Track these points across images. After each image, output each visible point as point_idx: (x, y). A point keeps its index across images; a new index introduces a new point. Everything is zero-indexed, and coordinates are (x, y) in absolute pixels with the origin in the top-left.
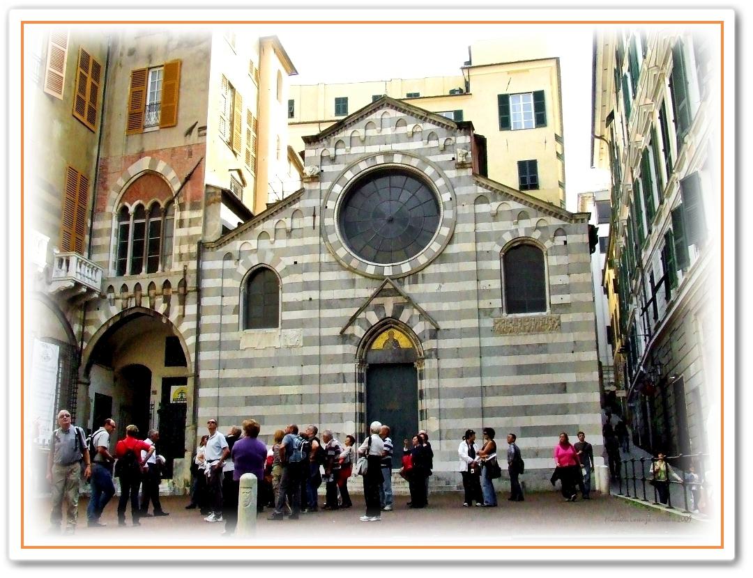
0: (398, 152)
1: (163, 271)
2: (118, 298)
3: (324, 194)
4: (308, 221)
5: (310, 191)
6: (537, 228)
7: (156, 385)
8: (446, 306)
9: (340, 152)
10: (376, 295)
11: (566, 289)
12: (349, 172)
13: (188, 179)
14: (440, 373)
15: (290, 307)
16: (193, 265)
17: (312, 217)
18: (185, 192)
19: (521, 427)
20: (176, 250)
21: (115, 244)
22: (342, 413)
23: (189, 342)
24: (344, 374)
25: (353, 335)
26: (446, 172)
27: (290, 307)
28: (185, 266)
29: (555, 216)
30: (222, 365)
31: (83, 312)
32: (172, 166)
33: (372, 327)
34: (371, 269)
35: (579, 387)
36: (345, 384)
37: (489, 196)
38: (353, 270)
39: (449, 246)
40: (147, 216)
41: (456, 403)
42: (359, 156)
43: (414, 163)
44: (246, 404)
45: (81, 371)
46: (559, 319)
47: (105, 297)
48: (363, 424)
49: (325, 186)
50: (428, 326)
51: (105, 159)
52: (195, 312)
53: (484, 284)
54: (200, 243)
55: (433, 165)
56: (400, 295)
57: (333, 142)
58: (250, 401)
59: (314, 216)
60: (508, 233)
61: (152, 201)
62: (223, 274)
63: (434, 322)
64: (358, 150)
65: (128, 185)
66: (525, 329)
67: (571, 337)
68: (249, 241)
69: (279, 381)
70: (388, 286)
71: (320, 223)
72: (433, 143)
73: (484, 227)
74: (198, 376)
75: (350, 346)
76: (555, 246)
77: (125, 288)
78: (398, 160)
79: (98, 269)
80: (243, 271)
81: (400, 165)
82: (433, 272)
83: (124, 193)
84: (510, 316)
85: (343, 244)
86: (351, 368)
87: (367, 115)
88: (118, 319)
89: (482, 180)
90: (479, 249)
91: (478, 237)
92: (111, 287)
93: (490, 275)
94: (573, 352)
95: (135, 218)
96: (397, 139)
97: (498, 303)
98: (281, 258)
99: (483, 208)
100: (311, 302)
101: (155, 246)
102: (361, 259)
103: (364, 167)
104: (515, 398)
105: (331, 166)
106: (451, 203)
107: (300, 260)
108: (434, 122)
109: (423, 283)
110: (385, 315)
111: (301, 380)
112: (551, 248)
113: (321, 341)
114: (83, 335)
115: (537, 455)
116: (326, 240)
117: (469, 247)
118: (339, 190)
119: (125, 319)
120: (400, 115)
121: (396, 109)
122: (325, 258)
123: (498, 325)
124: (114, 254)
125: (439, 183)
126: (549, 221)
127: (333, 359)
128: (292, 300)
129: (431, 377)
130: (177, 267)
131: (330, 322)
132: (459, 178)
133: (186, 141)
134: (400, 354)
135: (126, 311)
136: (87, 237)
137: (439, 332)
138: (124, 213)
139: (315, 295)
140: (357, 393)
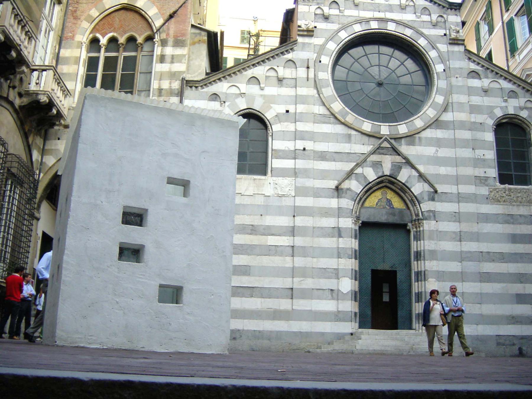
3: (317, 49)
4: (302, 72)
5: (304, 44)
8: (443, 170)
9: (334, 12)
10: (374, 152)
12: (343, 31)
13: (171, 16)
14: (441, 235)
18: (168, 29)
20: (155, 85)
21: (82, 73)
22: (337, 270)
25: (349, 189)
33: (370, 183)
34: (367, 126)
36: (340, 239)
37: (480, 73)
40: (121, 49)
42: (354, 19)
43: (408, 32)
49: (317, 41)
50: (427, 187)
53: (479, 153)
59: (308, 68)
63: (432, 186)
65: (102, 16)
66: (517, 200)
70: (386, 145)
71: (315, 75)
72: (426, 18)
73: (476, 100)
78: (391, 28)
83: (97, 24)
85: (338, 99)
91: (474, 109)
93: (482, 144)
95: (107, 50)
97: (493, 173)
98: (272, 105)
99: (475, 83)
100: (305, 152)
103: (358, 29)
106: (444, 73)
109: (420, 145)
110: (383, 172)
111: (293, 231)
113: (317, 193)
117: (462, 116)
118: (333, 47)
125: (432, 54)
127: (326, 213)
128: (284, 149)
131: (324, 175)
134: (394, 215)
137: (436, 196)
139: (309, 145)
140: (354, 250)
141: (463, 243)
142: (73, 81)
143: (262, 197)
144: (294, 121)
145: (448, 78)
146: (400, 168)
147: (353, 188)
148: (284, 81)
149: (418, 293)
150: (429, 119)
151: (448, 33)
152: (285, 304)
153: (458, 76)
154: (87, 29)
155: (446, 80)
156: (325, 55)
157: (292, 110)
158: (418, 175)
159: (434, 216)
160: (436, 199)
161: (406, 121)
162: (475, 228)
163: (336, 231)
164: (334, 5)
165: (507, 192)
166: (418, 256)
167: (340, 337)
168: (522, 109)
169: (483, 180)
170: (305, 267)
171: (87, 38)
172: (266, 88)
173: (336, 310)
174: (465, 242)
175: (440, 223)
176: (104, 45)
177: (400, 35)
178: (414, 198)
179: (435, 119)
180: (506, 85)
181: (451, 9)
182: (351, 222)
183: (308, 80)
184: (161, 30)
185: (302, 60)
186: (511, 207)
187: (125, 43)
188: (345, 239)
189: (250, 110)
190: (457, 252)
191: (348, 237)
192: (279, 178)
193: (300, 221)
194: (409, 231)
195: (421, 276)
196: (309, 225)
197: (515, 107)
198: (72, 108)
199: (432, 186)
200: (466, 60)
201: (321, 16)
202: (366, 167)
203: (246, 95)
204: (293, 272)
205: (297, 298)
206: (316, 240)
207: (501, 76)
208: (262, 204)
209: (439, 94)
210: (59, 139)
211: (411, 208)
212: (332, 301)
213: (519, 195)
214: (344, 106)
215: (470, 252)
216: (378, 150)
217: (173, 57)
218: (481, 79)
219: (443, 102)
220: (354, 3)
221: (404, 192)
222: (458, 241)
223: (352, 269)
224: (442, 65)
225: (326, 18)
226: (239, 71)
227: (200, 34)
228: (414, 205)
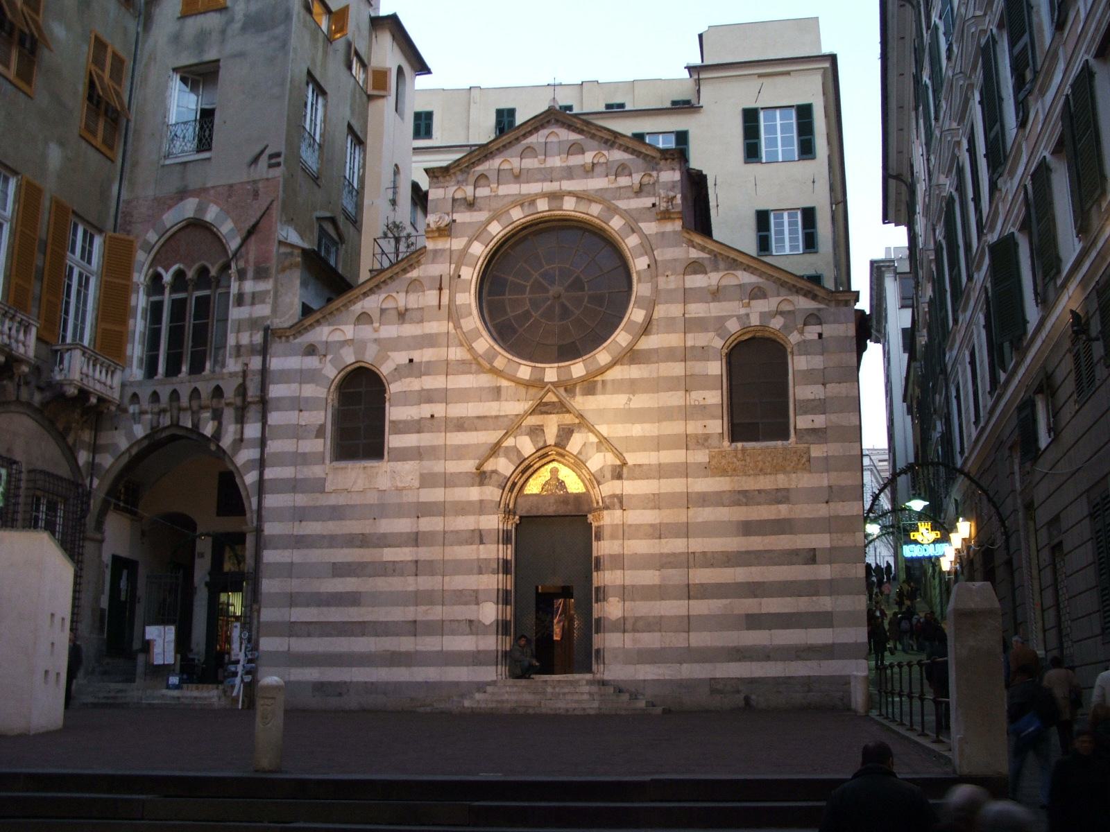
0: (570, 193)
1: (213, 372)
3: (455, 257)
4: (431, 297)
5: (436, 252)
6: (779, 313)
8: (637, 430)
9: (483, 192)
10: (533, 412)
13: (251, 232)
14: (624, 531)
16: (256, 363)
17: (438, 292)
18: (247, 253)
20: (231, 340)
21: (142, 329)
22: (476, 591)
23: (250, 478)
24: (480, 531)
25: (495, 472)
26: (642, 225)
29: (805, 295)
31: (93, 433)
32: (228, 213)
33: (525, 459)
34: (525, 371)
36: (482, 547)
37: (706, 263)
40: (190, 288)
41: (649, 577)
43: (595, 209)
44: (334, 576)
45: (90, 520)
47: (125, 411)
48: (509, 607)
49: (457, 244)
51: (128, 202)
52: (259, 435)
54: (266, 329)
55: (625, 214)
56: (568, 412)
58: (340, 570)
59: (440, 289)
60: (735, 318)
61: (196, 266)
63: (619, 455)
65: (162, 240)
68: (341, 327)
70: (551, 398)
72: (624, 181)
73: (697, 310)
74: (262, 531)
76: (804, 341)
77: (155, 397)
78: (569, 205)
80: (331, 372)
81: (573, 213)
82: (619, 377)
83: (158, 252)
88: (146, 443)
89: (698, 239)
90: (689, 344)
91: (690, 325)
92: (135, 398)
94: (827, 502)
96: (569, 173)
97: (716, 426)
101: (201, 334)
102: (510, 357)
105: (468, 214)
109: (603, 393)
110: (545, 441)
112: (798, 344)
113: (447, 481)
114: (93, 467)
116: (458, 326)
117: (673, 340)
118: (479, 250)
119: (156, 444)
120: (574, 136)
122: (456, 353)
124: (140, 347)
125: (631, 242)
126: (796, 303)
131: (460, 452)
132: (663, 234)
138: (155, 283)
139: (439, 410)
140: (501, 561)
141: (663, 541)
147: (501, 470)
151: (657, 204)
153: (669, 273)
154: (144, 263)
158: (596, 440)
159: (621, 502)
160: (625, 476)
161: (584, 358)
163: (477, 535)
164: (482, 182)
167: (481, 687)
170: (433, 590)
171: (146, 275)
172: (382, 327)
173: (475, 650)
174: (666, 540)
177: (583, 215)
178: (592, 477)
181: (666, 159)
183: (440, 308)
184: (238, 255)
185: (432, 278)
186: (744, 478)
187: (195, 277)
188: (488, 546)
190: (656, 554)
195: (601, 594)
196: (438, 529)
197: (762, 315)
199: (619, 455)
200: (684, 245)
201: (463, 202)
202: (521, 435)
203: (355, 341)
206: (448, 549)
208: (376, 502)
209: (639, 307)
210: (116, 429)
212: (470, 637)
215: (674, 554)
216: (539, 408)
217: (254, 295)
218: (706, 273)
220: (513, 174)
223: (498, 590)
226: (343, 306)
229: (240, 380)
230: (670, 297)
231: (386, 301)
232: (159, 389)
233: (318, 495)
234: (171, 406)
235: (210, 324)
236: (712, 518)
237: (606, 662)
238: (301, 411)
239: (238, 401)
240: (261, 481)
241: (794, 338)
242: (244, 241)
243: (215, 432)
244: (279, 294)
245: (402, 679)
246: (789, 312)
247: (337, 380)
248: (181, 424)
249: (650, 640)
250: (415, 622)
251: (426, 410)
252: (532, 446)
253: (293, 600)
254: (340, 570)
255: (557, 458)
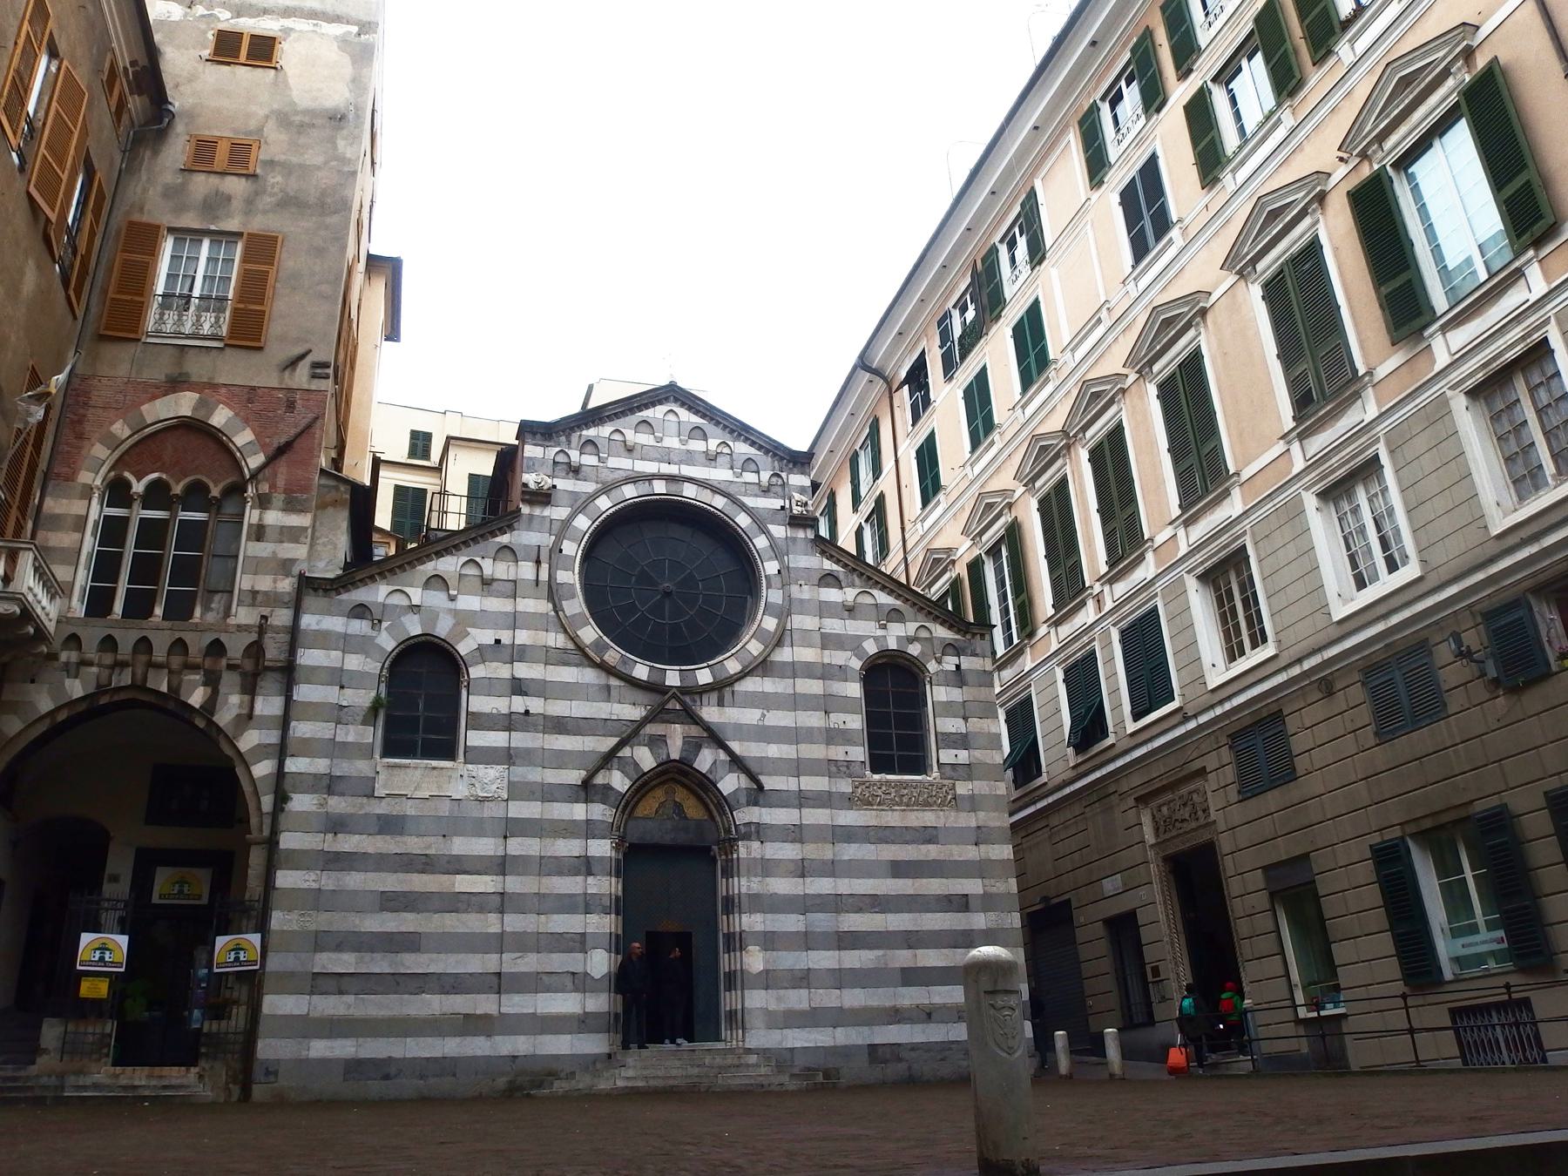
0: (691, 480)
2: (90, 664)
3: (556, 527)
4: (526, 570)
7: (120, 864)
8: (773, 751)
9: (589, 460)
11: (962, 741)
12: (604, 497)
14: (767, 868)
15: (481, 722)
16: (282, 617)
18: (275, 475)
19: (903, 969)
20: (244, 582)
22: (584, 935)
23: (262, 769)
24: (587, 857)
25: (608, 788)
27: (481, 722)
28: (264, 617)
30: (336, 825)
32: (246, 421)
33: (645, 774)
34: (641, 671)
35: (988, 902)
36: (590, 880)
37: (841, 577)
38: (603, 667)
39: (778, 650)
41: (791, 923)
42: (623, 474)
43: (719, 502)
44: (383, 909)
46: (953, 788)
47: (53, 657)
49: (559, 513)
51: (84, 379)
53: (837, 719)
57: (575, 437)
58: (392, 902)
59: (538, 562)
62: (346, 643)
63: (753, 777)
64: (623, 463)
66: (902, 800)
67: (968, 820)
69: (459, 866)
70: (674, 705)
72: (750, 477)
73: (834, 626)
74: (278, 843)
75: (602, 806)
77: (109, 643)
78: (689, 491)
79: (56, 593)
80: (388, 642)
84: (876, 777)
85: (591, 620)
86: (602, 848)
87: (640, 408)
88: (82, 707)
90: (826, 661)
91: (828, 641)
92: (74, 641)
93: (844, 704)
96: (689, 457)
97: (859, 753)
98: (469, 629)
99: (832, 595)
101: (187, 571)
103: (630, 492)
104: (891, 917)
106: (778, 579)
107: (506, 636)
108: (753, 444)
110: (668, 755)
111: (502, 866)
113: (548, 794)
115: (930, 1017)
117: (807, 654)
118: (583, 523)
121: (690, 409)
122: (556, 640)
123: (859, 790)
125: (761, 542)
126: (933, 630)
129: (749, 874)
130: (244, 615)
131: (561, 760)
133: (282, 380)
135: (106, 692)
136: (30, 525)
138: (117, 492)
139: (536, 705)
140: (613, 897)
141: (808, 880)
142: (69, 564)
143: (448, 802)
144: (509, 660)
145: (784, 585)
146: (698, 747)
148: (495, 584)
149: (730, 972)
150: (752, 658)
151: (787, 506)
152: (485, 1004)
153: (803, 583)
154: (104, 462)
155: (782, 588)
156: (569, 539)
157: (506, 640)
158: (728, 759)
159: (758, 832)
160: (761, 802)
162: (826, 852)
164: (589, 448)
165: (884, 788)
166: (730, 905)
168: (911, 640)
169: (842, 766)
173: (581, 1012)
175: (768, 845)
176: (140, 496)
179: (761, 659)
180: (883, 598)
182: (609, 847)
184: (260, 476)
186: (890, 813)
189: (428, 638)
191: (603, 875)
192: (481, 766)
193: (517, 846)
194: (714, 860)
195: (736, 942)
197: (899, 638)
198: (64, 620)
199: (753, 777)
204: (499, 943)
205: (508, 992)
206: (546, 880)
207: (877, 583)
208: (447, 814)
210: (33, 681)
211: (718, 819)
213: (906, 791)
214: (602, 634)
218: (841, 588)
219: (776, 630)
221: (706, 790)
222: (800, 877)
224: (776, 562)
225: (575, 471)
227: (337, 488)
228: (722, 813)
229: (254, 637)
230: (803, 607)
231: (466, 567)
232: (116, 634)
233: (365, 800)
234: (133, 659)
235: (205, 559)
236: (859, 856)
237: (748, 1026)
238: (342, 687)
239: (249, 665)
240: (280, 774)
241: (932, 666)
242: (271, 460)
243: (206, 702)
244: (317, 534)
245: (479, 1053)
246: (926, 638)
247: (394, 653)
248: (149, 685)
249: (798, 999)
250: (499, 974)
251: (519, 704)
252: (652, 759)
253: (321, 941)
254: (392, 902)
255: (677, 776)
